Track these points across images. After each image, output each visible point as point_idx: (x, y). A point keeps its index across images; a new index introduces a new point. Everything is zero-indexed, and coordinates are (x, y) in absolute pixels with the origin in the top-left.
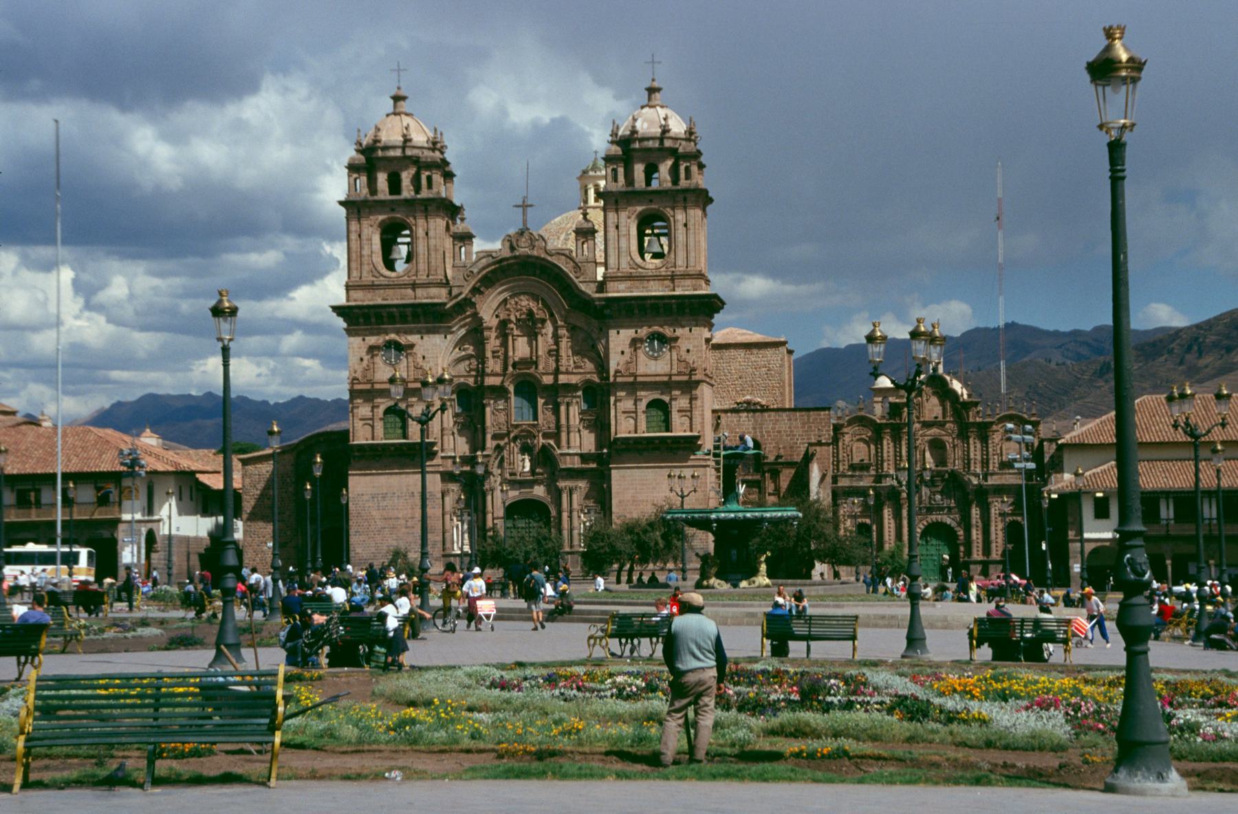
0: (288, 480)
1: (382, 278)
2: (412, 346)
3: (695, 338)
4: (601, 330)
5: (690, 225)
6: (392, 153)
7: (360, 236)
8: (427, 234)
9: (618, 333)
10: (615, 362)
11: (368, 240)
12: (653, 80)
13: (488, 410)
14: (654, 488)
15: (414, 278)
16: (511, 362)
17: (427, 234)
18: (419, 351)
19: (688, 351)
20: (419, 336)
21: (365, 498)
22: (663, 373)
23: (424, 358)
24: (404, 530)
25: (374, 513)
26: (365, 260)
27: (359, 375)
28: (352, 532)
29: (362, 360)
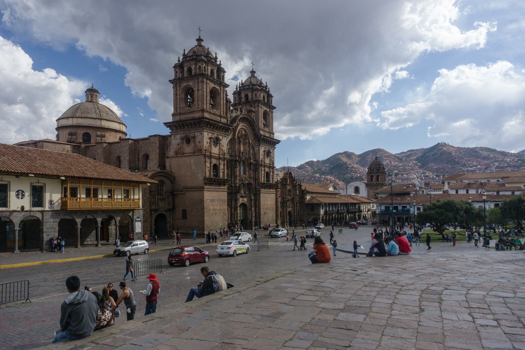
0: (147, 191)
10: (261, 157)
12: (253, 69)
20: (222, 137)
21: (209, 201)
24: (218, 214)
25: (211, 207)
28: (205, 215)
29: (207, 142)
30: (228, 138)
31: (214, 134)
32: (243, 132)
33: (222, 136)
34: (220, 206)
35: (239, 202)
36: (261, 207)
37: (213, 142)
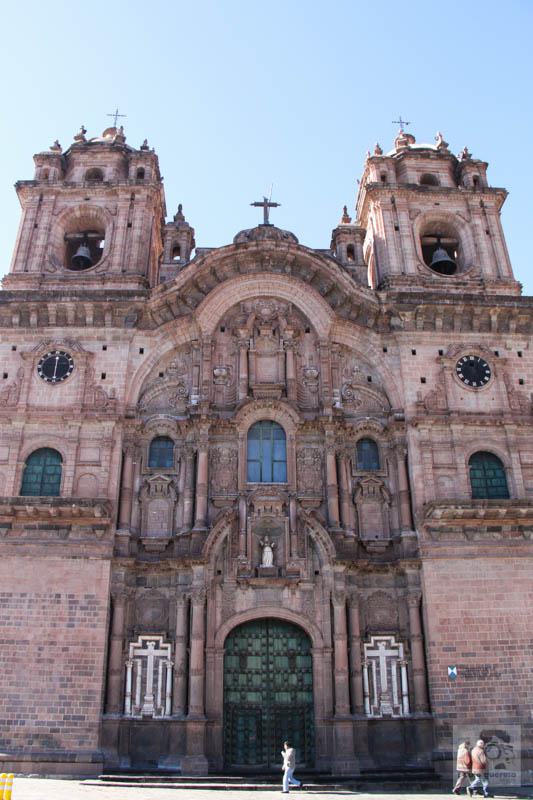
2: (91, 355)
4: (385, 350)
7: (36, 226)
8: (130, 225)
9: (414, 353)
13: (202, 457)
14: (499, 598)
17: (130, 225)
18: (99, 367)
19: (521, 382)
22: (488, 410)
23: (104, 376)
24: (32, 665)
26: (38, 251)
29: (6, 376)
32: (266, 311)
33: (100, 339)
34: (55, 625)
35: (228, 614)
36: (433, 635)
37: (39, 370)
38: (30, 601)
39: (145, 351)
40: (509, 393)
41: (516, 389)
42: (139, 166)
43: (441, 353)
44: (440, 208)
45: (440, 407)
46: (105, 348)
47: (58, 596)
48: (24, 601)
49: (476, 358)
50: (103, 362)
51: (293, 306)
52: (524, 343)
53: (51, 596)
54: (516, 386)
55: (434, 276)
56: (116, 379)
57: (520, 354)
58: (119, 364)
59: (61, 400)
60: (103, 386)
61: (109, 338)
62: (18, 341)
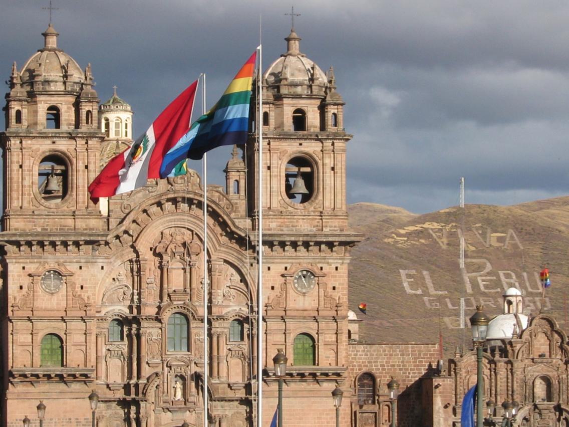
1: (42, 207)
3: (340, 277)
4: (252, 265)
5: (337, 169)
6: (53, 87)
7: (21, 166)
8: (87, 167)
9: (269, 269)
11: (29, 171)
14: (301, 419)
15: (74, 209)
16: (165, 292)
17: (87, 167)
18: (78, 280)
19: (334, 288)
22: (310, 308)
23: (82, 287)
26: (26, 190)
27: (18, 302)
29: (21, 288)
30: (111, 263)
31: (45, 263)
38: (55, 422)
39: (104, 267)
40: (325, 296)
41: (330, 294)
42: (87, 109)
43: (286, 268)
44: (302, 149)
45: (280, 306)
46: (81, 268)
47: (70, 419)
48: (52, 423)
49: (308, 271)
50: (81, 278)
51: (196, 234)
52: (341, 261)
53: (66, 419)
54: (330, 290)
55: (290, 209)
56: (89, 290)
57: (337, 268)
58: (90, 280)
59: (58, 304)
60: (83, 294)
61: (83, 261)
62: (27, 263)
